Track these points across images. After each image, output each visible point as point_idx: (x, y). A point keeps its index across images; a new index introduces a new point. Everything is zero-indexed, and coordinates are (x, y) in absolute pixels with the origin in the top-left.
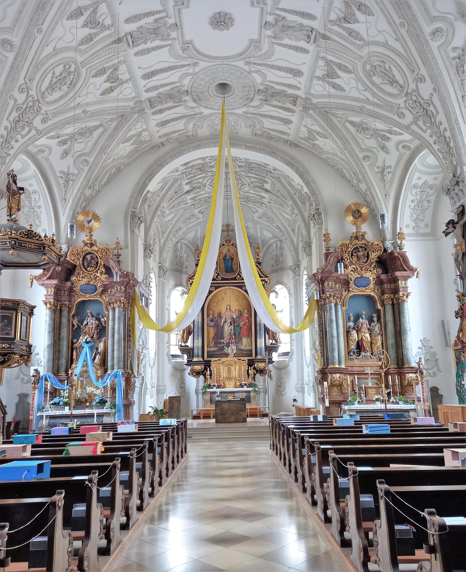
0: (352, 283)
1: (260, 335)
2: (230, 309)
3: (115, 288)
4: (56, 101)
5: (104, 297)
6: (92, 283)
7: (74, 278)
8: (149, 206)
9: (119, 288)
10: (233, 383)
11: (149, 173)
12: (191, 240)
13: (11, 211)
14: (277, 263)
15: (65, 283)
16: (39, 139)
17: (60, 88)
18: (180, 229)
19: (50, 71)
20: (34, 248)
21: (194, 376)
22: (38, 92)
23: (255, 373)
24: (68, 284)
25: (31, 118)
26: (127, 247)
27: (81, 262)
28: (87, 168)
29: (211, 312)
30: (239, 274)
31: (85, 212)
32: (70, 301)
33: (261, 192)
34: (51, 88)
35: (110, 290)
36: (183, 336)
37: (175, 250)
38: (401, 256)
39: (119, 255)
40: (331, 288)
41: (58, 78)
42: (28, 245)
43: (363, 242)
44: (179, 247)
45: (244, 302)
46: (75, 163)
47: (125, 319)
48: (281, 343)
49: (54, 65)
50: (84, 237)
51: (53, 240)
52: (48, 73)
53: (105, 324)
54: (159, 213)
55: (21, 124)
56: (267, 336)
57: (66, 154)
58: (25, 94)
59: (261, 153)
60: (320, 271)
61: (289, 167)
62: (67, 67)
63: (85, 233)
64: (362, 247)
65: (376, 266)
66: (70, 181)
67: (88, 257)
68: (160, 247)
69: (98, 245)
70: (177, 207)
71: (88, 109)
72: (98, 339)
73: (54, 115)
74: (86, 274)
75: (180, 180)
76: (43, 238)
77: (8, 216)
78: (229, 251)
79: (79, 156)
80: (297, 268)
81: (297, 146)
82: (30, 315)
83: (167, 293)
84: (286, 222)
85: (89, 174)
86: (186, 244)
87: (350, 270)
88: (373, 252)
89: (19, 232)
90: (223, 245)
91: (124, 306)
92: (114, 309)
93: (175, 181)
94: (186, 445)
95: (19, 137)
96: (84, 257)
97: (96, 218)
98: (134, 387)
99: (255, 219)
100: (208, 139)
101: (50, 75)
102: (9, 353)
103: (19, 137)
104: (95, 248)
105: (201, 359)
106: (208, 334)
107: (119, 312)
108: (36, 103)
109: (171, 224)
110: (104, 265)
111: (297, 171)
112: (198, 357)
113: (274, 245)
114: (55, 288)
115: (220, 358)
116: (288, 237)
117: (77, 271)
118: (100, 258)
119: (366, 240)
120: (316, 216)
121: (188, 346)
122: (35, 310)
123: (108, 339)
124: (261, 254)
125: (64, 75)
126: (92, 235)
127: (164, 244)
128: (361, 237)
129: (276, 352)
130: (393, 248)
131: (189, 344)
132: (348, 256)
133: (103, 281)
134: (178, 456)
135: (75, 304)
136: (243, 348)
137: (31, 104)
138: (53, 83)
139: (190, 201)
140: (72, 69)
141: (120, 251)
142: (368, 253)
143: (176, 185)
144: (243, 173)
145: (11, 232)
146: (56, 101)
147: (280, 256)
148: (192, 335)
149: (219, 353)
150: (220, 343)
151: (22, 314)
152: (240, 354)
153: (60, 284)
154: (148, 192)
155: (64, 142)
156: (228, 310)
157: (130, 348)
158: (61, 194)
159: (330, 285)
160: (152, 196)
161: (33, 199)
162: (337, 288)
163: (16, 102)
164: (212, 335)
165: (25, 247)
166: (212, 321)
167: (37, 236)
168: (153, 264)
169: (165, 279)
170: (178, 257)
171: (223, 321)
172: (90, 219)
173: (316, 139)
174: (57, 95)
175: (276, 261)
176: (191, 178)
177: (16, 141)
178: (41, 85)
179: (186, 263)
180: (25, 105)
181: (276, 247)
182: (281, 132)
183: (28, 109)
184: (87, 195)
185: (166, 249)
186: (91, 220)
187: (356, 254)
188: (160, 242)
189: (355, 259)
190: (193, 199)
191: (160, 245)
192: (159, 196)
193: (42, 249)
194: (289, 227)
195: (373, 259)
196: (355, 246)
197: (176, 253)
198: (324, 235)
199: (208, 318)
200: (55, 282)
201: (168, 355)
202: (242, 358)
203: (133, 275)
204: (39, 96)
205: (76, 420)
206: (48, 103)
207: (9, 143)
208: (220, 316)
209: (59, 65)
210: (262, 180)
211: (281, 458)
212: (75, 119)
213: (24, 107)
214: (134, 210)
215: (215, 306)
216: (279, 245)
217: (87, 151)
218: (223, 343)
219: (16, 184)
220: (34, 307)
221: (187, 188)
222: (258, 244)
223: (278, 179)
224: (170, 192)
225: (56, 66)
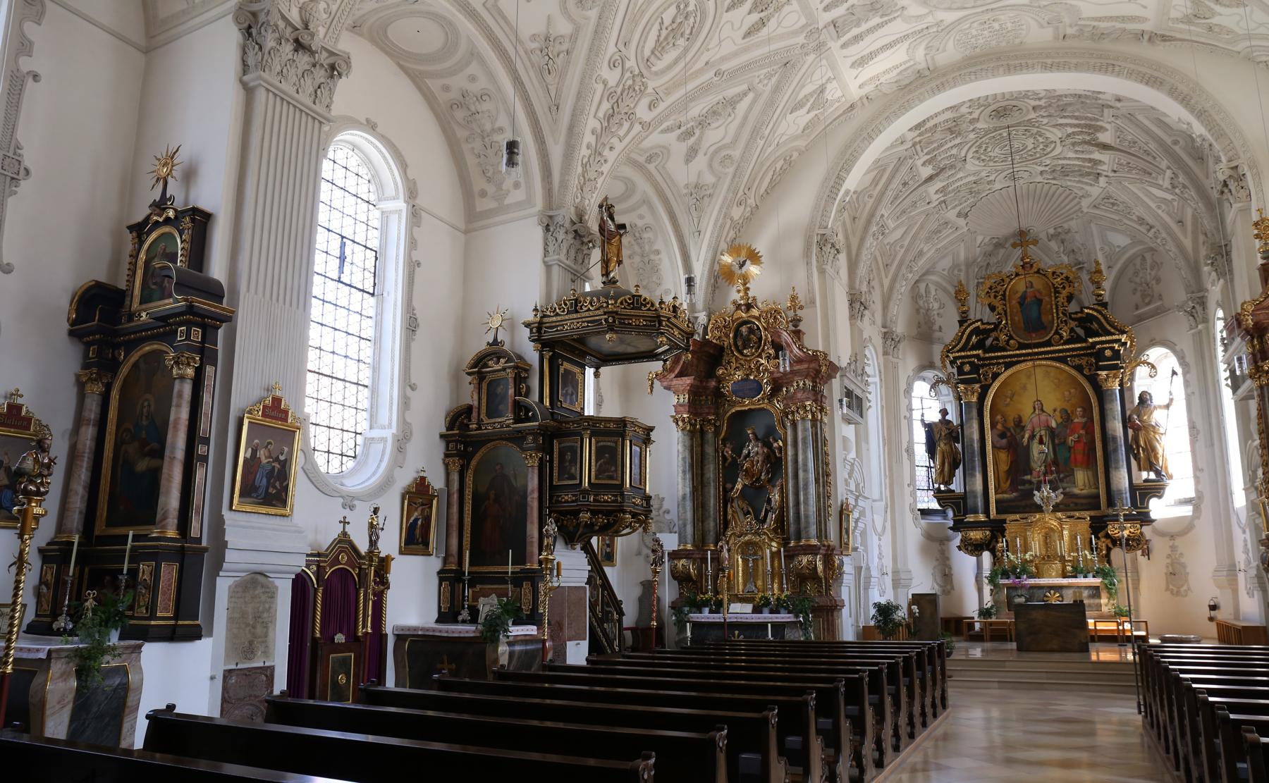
1: (1117, 461)
2: (1042, 410)
3: (795, 384)
4: (669, 67)
5: (775, 402)
6: (752, 378)
7: (721, 372)
8: (854, 218)
9: (801, 384)
10: (1057, 565)
11: (847, 157)
12: (945, 273)
13: (607, 266)
14: (1147, 301)
15: (707, 382)
16: (647, 136)
17: (674, 45)
18: (921, 253)
19: (656, 20)
20: (644, 325)
21: (971, 553)
22: (640, 60)
23: (1110, 545)
24: (713, 383)
25: (632, 105)
26: (813, 302)
27: (731, 341)
28: (731, 170)
29: (999, 417)
30: (1057, 333)
31: (734, 249)
32: (717, 414)
33: (1091, 152)
34: (660, 48)
35: (784, 389)
36: (942, 471)
37: (915, 296)
39: (796, 321)
41: (670, 28)
42: (634, 322)
44: (922, 291)
45: (1072, 391)
46: (710, 166)
47: (817, 441)
48: (1171, 477)
49: (660, 10)
50: (735, 295)
51: (674, 307)
52: (652, 25)
53: (781, 453)
54: (875, 228)
55: (616, 119)
56: (1134, 463)
57: (692, 153)
58: (619, 70)
59: (1081, 71)
60: (1251, 308)
61: (1152, 87)
62: (682, 7)
63: (735, 287)
66: (705, 198)
67: (744, 329)
68: (883, 295)
69: (760, 305)
70: (910, 212)
71: (724, 67)
72: (770, 481)
73: (668, 92)
74: (742, 362)
75: (911, 158)
76: (658, 306)
77: (603, 275)
78: (1032, 287)
79: (716, 152)
80: (1197, 306)
81: (1165, 38)
82: (645, 443)
83: (903, 386)
84: (1159, 207)
85: (737, 179)
86: (937, 284)
89: (619, 301)
90: (1017, 275)
91: (813, 416)
92: (794, 424)
93: (901, 161)
94: (943, 691)
95: (615, 141)
96: (737, 332)
97: (754, 257)
98: (841, 574)
99: (1085, 210)
100: (959, 69)
101: (657, 26)
102: (614, 511)
103: (615, 141)
104: (755, 312)
105: (982, 518)
106: (996, 464)
107: (805, 430)
108: (638, 79)
109: (902, 247)
110: (772, 341)
111: (1173, 92)
112: (976, 512)
113: (1138, 261)
114: (690, 392)
115: (1026, 515)
116: (1169, 239)
117: (726, 358)
118: (765, 329)
120: (1232, 185)
121: (953, 491)
122: (653, 435)
123: (787, 481)
124: (1107, 285)
125: (679, 20)
126: (748, 289)
127: (891, 288)
129: (1160, 497)
131: (957, 486)
133: (772, 373)
134: (923, 714)
135: (726, 418)
136: (1076, 491)
137: (630, 82)
138: (662, 39)
139: (937, 196)
140: (691, 8)
141: (799, 313)
143: (904, 169)
144: (1045, 121)
145: (607, 303)
146: (669, 67)
147: (1154, 282)
148: (961, 466)
149: (1023, 503)
150: (1024, 482)
151: (631, 441)
152: (1069, 505)
153: (699, 383)
154: (847, 192)
155: (689, 133)
156: (1037, 412)
157: (829, 497)
158: (692, 224)
160: (857, 198)
161: (646, 241)
163: (606, 85)
164: (1004, 467)
165: (630, 324)
166: (1002, 436)
167: (648, 303)
168: (871, 329)
169: (898, 358)
170: (922, 311)
171: (1027, 436)
172: (742, 260)
173: (1214, 14)
174: (669, 57)
175: (1144, 296)
176: (934, 150)
177: (611, 148)
178: (643, 47)
179: (939, 322)
180: (621, 86)
181: (1141, 264)
182: (1123, 19)
183: (626, 92)
184: (736, 218)
185: (897, 296)
186: (744, 262)
188: (882, 286)
190: (942, 190)
191: (883, 293)
192: (870, 196)
193: (657, 325)
194: (1170, 215)
197: (916, 302)
198: (1256, 224)
199: (994, 430)
200: (688, 381)
201: (912, 511)
202: (1077, 514)
203: (826, 355)
204: (641, 66)
205: (737, 632)
206: (656, 73)
207: (600, 154)
208: (1019, 424)
209: (669, 7)
210: (1090, 126)
211: (1159, 734)
212: (704, 90)
213: (619, 90)
214: (822, 232)
215: (1007, 405)
216: (1149, 261)
217: (728, 140)
218: (1030, 482)
219: (612, 219)
220: (651, 429)
221: (927, 171)
222: (1097, 263)
223: (1131, 117)
224: (893, 186)
225: (665, 10)
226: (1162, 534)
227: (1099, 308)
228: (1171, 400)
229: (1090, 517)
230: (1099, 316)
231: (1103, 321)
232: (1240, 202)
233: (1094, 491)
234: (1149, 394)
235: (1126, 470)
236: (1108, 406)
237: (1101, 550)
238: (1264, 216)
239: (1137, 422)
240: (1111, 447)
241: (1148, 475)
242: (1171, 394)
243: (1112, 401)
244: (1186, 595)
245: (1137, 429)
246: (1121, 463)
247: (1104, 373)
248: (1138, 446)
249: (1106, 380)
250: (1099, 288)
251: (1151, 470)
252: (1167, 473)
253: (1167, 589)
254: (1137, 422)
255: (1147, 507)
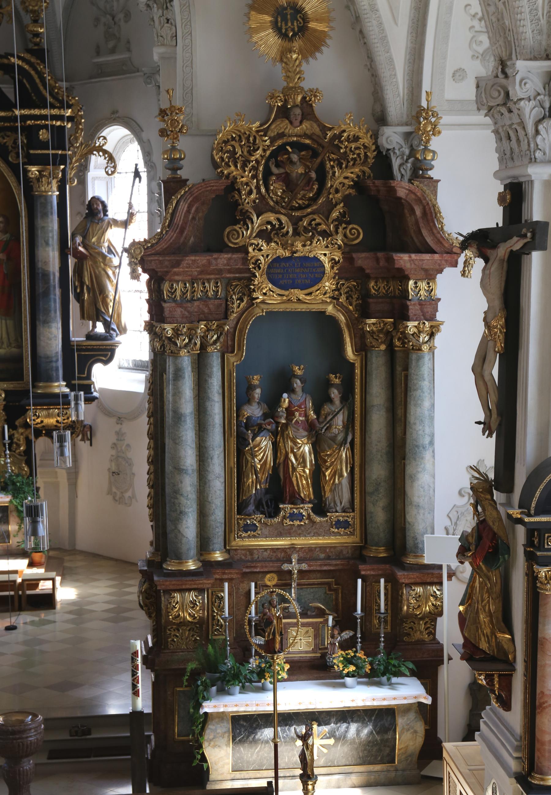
0: (260, 279)
1: (47, 311)
14: (111, 44)
38: (419, 201)
40: (180, 305)
43: (306, 125)
56: (74, 306)
64: (298, 146)
65: (343, 215)
87: (256, 230)
88: (340, 165)
119: (316, 120)
128: (298, 111)
130: (407, 152)
132: (255, 177)
142: (322, 166)
147: (121, 16)
159: (178, 293)
162: (211, 293)
187: (282, 171)
189: (277, 188)
195: (337, 191)
196: (280, 142)
198: (163, 113)
226: (108, 413)
227: (33, 60)
228: (131, 215)
229: (6, 391)
230: (33, 73)
231: (38, 81)
232: (163, 45)
233: (14, 350)
234: (103, 203)
235: (60, 325)
236: (39, 222)
237: (19, 446)
238: (173, 104)
239: (81, 249)
240: (40, 289)
241: (94, 326)
242: (131, 206)
243: (46, 215)
244: (130, 506)
245: (80, 258)
246: (52, 314)
247: (34, 169)
248: (82, 284)
249: (38, 179)
250: (35, 21)
251: (98, 320)
252: (119, 325)
253: (110, 492)
254: (81, 249)
255: (89, 377)
